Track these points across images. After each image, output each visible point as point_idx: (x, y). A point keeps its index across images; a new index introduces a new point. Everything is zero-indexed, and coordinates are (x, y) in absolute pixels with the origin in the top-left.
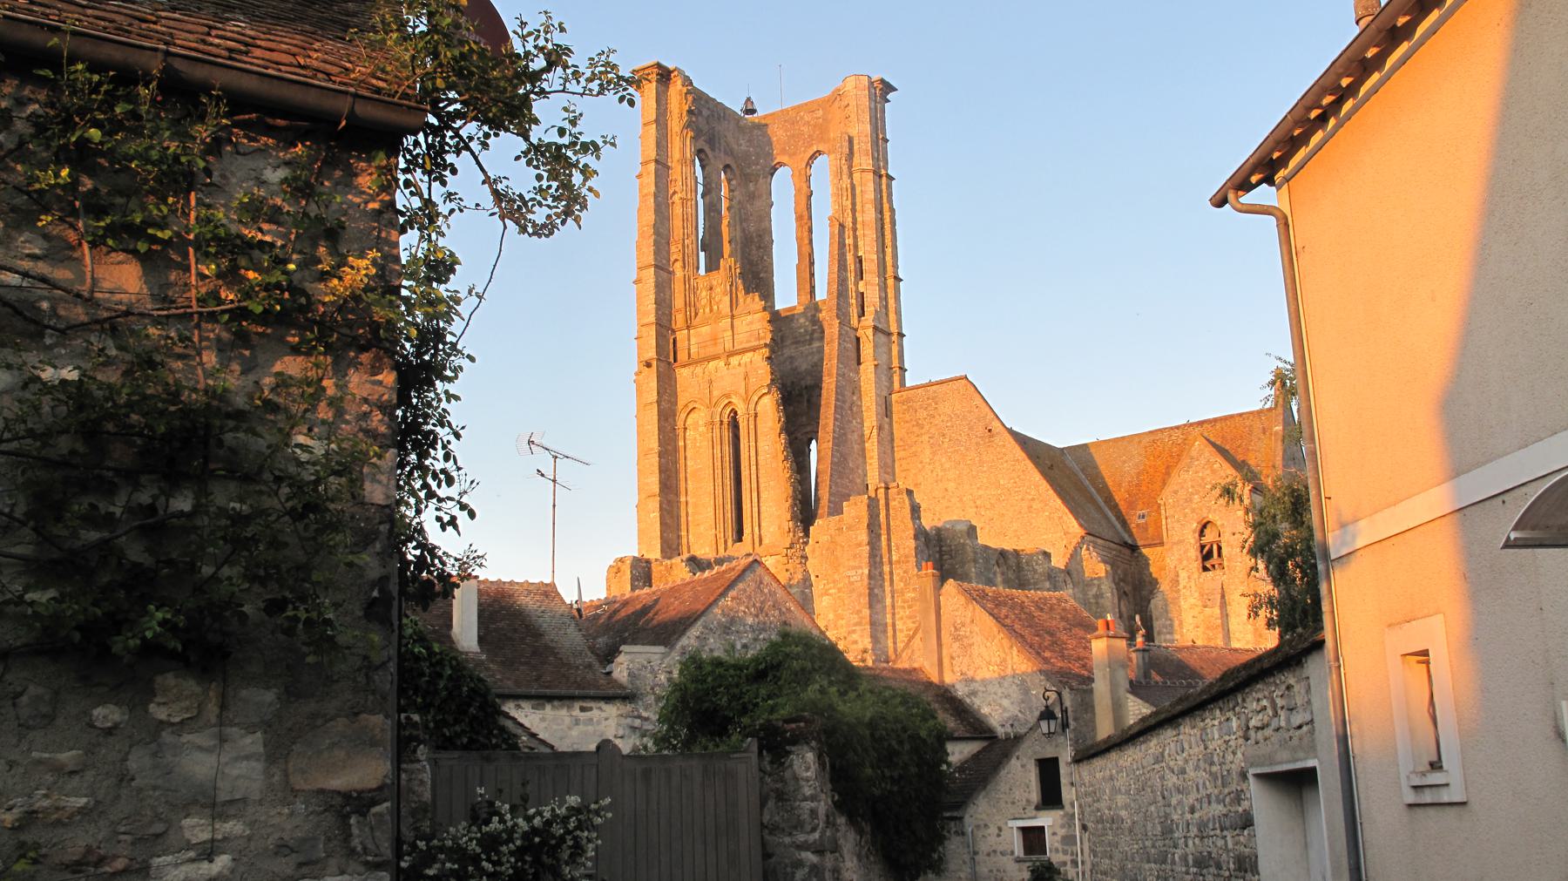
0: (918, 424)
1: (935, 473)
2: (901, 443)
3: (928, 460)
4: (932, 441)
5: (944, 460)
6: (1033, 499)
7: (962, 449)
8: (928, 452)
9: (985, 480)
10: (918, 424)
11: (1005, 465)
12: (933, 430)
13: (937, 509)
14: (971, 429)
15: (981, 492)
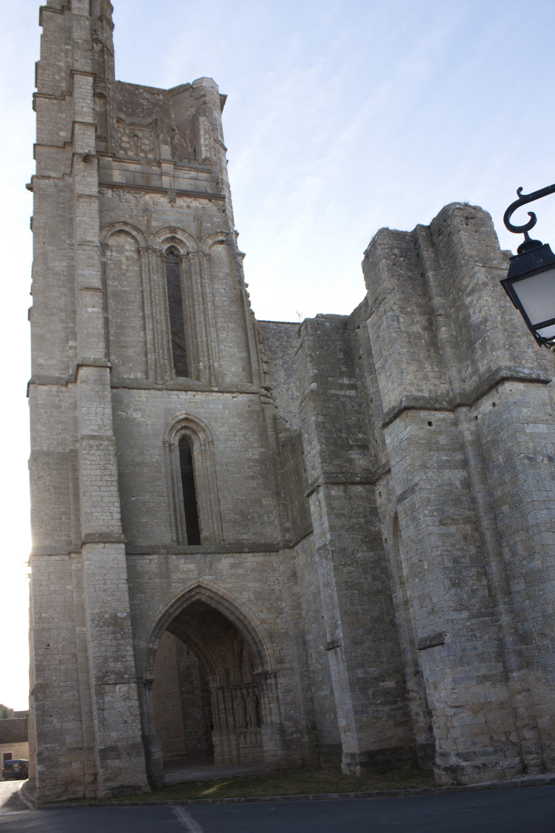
1: (290, 393)
3: (283, 380)
4: (285, 366)
8: (282, 373)
12: (287, 358)
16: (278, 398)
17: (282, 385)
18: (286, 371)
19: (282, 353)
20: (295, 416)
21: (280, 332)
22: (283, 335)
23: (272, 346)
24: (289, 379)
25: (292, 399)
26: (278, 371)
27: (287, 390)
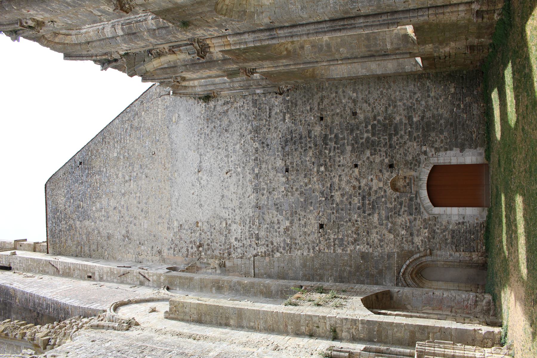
1: (103, 219)
2: (79, 247)
3: (93, 223)
5: (94, 208)
7: (89, 190)
8: (87, 223)
9: (112, 170)
11: (104, 151)
12: (74, 216)
13: (127, 219)
16: (108, 231)
19: (71, 220)
20: (122, 217)
21: (55, 218)
22: (56, 216)
23: (66, 227)
27: (101, 221)
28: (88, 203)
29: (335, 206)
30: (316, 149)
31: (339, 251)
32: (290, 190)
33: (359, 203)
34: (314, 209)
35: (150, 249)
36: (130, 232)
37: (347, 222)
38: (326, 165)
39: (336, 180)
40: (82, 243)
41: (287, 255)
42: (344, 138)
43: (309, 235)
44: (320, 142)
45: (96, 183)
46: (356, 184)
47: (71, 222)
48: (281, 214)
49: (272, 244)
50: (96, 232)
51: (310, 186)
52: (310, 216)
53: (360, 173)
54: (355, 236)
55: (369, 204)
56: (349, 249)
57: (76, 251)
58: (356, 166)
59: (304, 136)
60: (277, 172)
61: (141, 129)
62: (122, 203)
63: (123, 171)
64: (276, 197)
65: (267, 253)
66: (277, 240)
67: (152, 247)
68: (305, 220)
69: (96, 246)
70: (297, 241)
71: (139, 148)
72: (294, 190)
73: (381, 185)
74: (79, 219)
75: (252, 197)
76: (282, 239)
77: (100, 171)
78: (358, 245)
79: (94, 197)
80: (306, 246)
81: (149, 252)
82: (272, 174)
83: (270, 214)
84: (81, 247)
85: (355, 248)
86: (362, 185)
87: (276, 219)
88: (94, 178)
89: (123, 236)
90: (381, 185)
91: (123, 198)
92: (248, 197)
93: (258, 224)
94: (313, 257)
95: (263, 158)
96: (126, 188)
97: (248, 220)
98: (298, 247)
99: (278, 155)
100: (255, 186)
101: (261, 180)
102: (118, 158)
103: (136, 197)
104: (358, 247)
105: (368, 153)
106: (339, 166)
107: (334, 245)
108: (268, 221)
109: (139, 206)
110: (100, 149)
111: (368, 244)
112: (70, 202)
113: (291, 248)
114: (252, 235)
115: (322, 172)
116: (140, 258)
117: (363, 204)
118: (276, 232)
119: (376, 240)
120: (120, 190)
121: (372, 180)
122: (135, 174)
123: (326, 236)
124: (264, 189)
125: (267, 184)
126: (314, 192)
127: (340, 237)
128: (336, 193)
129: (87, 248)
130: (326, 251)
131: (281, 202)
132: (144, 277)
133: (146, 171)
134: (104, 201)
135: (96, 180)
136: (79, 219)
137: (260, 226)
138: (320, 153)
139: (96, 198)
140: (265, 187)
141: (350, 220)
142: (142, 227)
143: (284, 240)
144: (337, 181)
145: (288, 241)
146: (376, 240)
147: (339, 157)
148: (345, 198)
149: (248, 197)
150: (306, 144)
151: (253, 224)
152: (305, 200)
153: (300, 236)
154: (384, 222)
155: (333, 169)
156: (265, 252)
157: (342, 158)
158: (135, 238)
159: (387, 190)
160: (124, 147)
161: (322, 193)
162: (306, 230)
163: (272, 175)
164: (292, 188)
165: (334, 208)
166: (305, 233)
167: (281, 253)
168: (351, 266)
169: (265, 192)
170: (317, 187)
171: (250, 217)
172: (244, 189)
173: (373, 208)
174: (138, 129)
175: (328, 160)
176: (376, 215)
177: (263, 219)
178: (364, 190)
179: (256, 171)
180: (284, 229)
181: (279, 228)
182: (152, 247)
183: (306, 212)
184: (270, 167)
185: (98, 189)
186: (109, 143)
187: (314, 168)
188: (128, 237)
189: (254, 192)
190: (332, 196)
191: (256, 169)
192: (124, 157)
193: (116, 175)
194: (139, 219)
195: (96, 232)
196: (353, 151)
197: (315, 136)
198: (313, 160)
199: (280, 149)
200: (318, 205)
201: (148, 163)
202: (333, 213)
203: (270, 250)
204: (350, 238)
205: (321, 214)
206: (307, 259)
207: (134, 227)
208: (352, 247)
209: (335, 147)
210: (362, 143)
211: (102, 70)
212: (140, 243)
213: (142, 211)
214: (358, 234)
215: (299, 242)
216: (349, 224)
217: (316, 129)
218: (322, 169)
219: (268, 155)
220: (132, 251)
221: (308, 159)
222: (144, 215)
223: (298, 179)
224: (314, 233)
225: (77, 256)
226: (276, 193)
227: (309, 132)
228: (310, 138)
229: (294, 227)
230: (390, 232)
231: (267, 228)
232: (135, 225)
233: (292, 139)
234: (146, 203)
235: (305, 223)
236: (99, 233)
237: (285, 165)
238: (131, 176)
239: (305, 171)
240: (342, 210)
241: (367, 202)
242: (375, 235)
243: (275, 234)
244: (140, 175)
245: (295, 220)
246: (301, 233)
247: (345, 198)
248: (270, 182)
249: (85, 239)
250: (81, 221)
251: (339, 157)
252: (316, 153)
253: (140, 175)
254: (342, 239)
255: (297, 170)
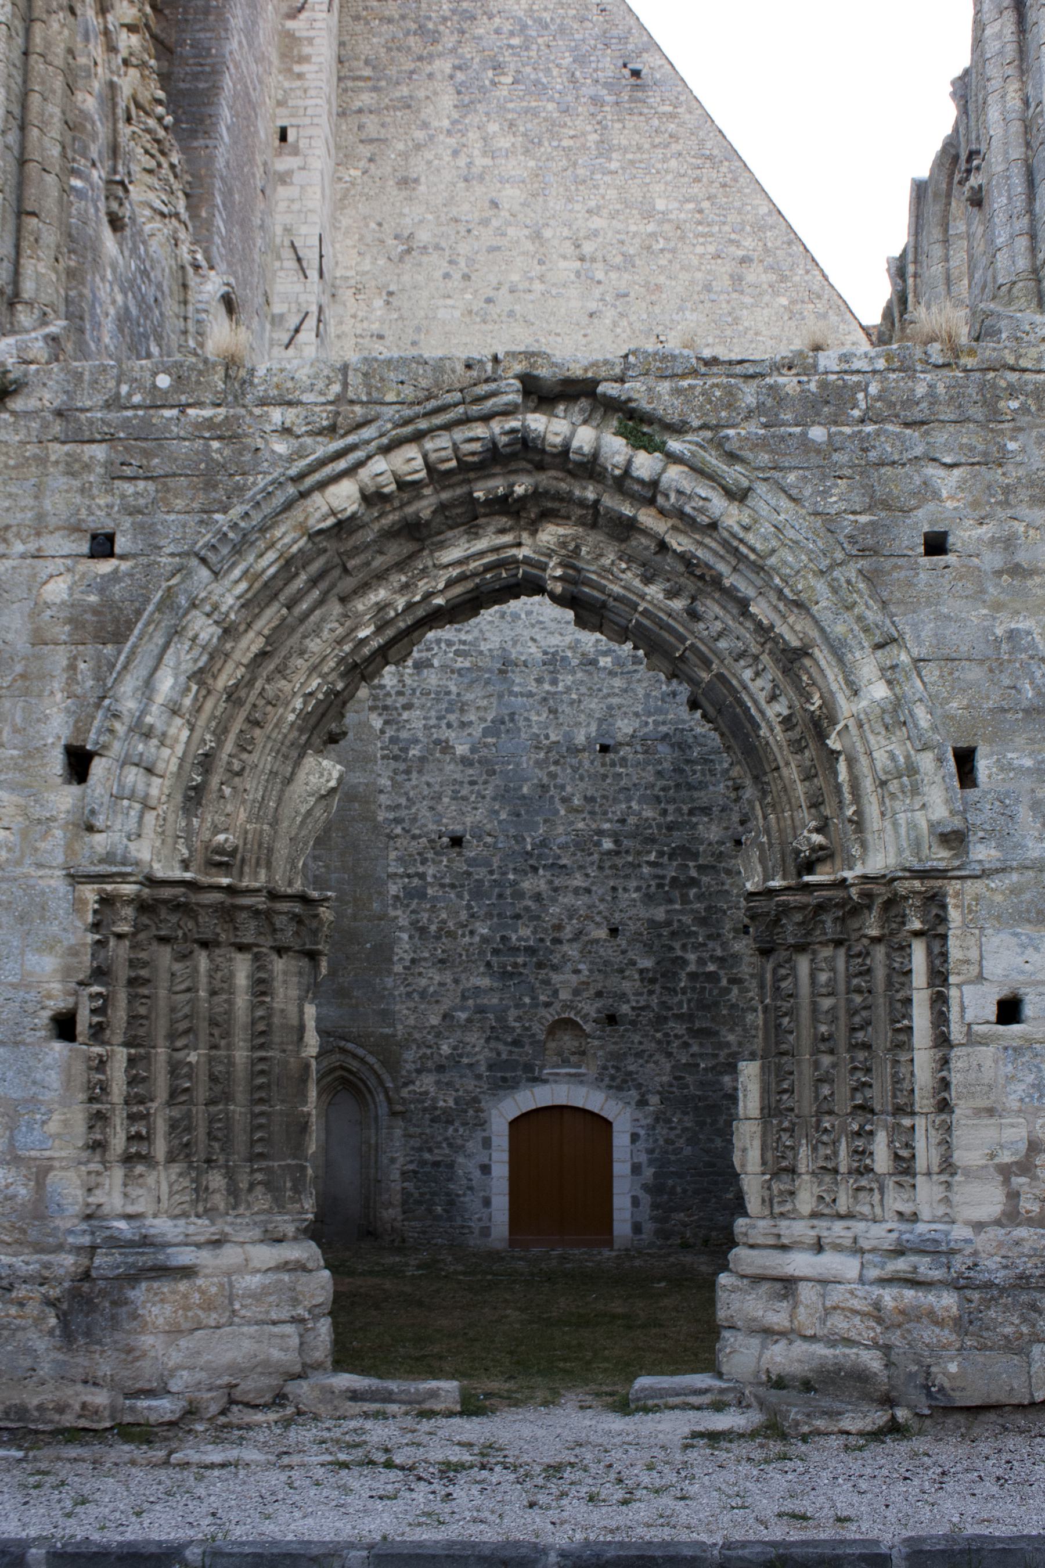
0: (421, 30)
1: (462, 161)
2: (367, 72)
3: (446, 123)
4: (460, 76)
5: (493, 128)
6: (744, 260)
7: (551, 106)
8: (447, 100)
9: (612, 194)
10: (421, 30)
11: (673, 163)
12: (467, 51)
13: (463, 248)
14: (581, 60)
15: (597, 223)
16: (423, 179)
17: (441, 137)
18: (459, 93)
19: (455, 37)
20: (469, 231)
23: (429, 18)
24: (464, 116)
25: (466, 180)
26: (436, 93)
27: (455, 153)
28: (510, 106)
29: (511, 877)
30: (659, 826)
31: (393, 889)
32: (555, 756)
33: (519, 939)
34: (500, 822)
35: (375, 327)
36: (425, 259)
37: (469, 907)
38: (617, 853)
39: (578, 881)
40: (383, 83)
41: (377, 748)
42: (685, 900)
43: (432, 808)
44: (678, 838)
45: (572, 133)
46: (567, 933)
47: (449, 41)
48: (486, 732)
49: (408, 707)
50: (420, 135)
51: (562, 812)
52: (480, 814)
53: (597, 941)
54: (433, 928)
55: (515, 965)
56: (399, 913)
57: (357, 59)
58: (614, 932)
59: (696, 794)
60: (601, 721)
61: (735, 295)
62: (511, 231)
63: (610, 234)
64: (534, 718)
65: (381, 693)
66: (415, 720)
67: (381, 337)
68: (473, 798)
69: (374, 135)
70: (414, 775)
71: (679, 289)
72: (552, 768)
73: (564, 995)
74: (459, 68)
75: (533, 649)
76: (420, 735)
77: (611, 149)
78: (411, 937)
79: (529, 126)
80: (403, 801)
81: (365, 324)
82: (593, 704)
83: (485, 702)
84: (369, 78)
85: (401, 929)
86: (565, 947)
87: (473, 718)
88: (589, 128)
89: (411, 235)
90: (564, 995)
91: (526, 232)
92: (533, 639)
93: (459, 665)
94: (374, 820)
95: (639, 681)
96: (555, 242)
97: (469, 638)
98: (400, 778)
99: (647, 723)
100: (564, 659)
101: (579, 675)
102: (648, 215)
103: (531, 279)
104: (405, 936)
105: (647, 963)
106: (614, 889)
107: (409, 876)
108: (469, 696)
109: (504, 290)
110: (679, 147)
111: (413, 961)
112: (512, 34)
113: (396, 758)
114: (429, 649)
115: (598, 844)
116: (346, 294)
117: (515, 950)
118: (439, 718)
119: (424, 982)
120: (552, 222)
121: (577, 972)
122: (600, 275)
123: (430, 855)
124: (554, 682)
125: (568, 690)
126: (546, 821)
127: (430, 891)
128: (542, 882)
129: (366, 99)
130: (393, 855)
131: (519, 730)
132: (297, 330)
133: (610, 314)
134: (516, 167)
135: (584, 134)
136: (459, 68)
137: (452, 672)
138: (652, 840)
139: (525, 135)
140: (561, 687)
141: (472, 916)
142: (441, 302)
143: (416, 741)
144: (576, 883)
145: (414, 752)
146: (424, 982)
147: (638, 889)
148: (530, 903)
149: (533, 639)
150: (674, 801)
151: (457, 653)
152: (524, 797)
153: (428, 784)
154: (471, 1002)
155: (608, 872)
156: (382, 687)
157: (635, 895)
158: (406, 278)
159: (551, 1010)
160: (682, 238)
161: (544, 843)
162: (446, 800)
163: (593, 706)
164: (556, 763)
165: (505, 874)
166: (438, 797)
167: (383, 732)
168: (354, 917)
169: (547, 687)
170: (561, 829)
171: (474, 643)
172: (553, 626)
173: (505, 975)
174: (737, 280)
175: (630, 859)
176: (485, 982)
177: (472, 682)
178: (552, 952)
179: (605, 662)
180: (447, 741)
181: (449, 726)
182: (381, 337)
183: (494, 799)
184: (615, 701)
185: (555, 143)
186: (697, 180)
187: (610, 821)
188: (409, 251)
189: (545, 653)
190: (535, 869)
191: (609, 659)
192: (653, 235)
193: (599, 207)
194: (463, 290)
195: (420, 135)
196: (653, 924)
197: (694, 827)
198: (632, 820)
199: (664, 729)
200: (512, 832)
201: (633, 318)
202: (491, 872)
203: (389, 702)
204: (426, 915)
205: (489, 840)
206: (367, 802)
207: (438, 274)
208: (403, 921)
209: (663, 877)
210: (671, 949)
211: (914, 180)
212: (390, 294)
213: (489, 300)
214: (438, 938)
215: (414, 782)
216: (464, 915)
217: (714, 828)
218: (608, 844)
219: (647, 696)
220: (367, 266)
221: (634, 805)
222: (475, 309)
223: (582, 779)
224: (438, 823)
225: (340, 62)
226: (543, 718)
227: (706, 811)
228: (691, 813)
229: (452, 767)
230: (445, 1016)
231: (448, 693)
232: (447, 276)
233: (688, 762)
234: (511, 314)
235: (465, 799)
236: (418, 147)
237: (621, 744)
238: (593, 260)
239: (604, 797)
240: (500, 896)
241: (520, 960)
242: (437, 978)
243: (433, 713)
244: (597, 292)
245: (471, 772)
246: (437, 788)
247: (530, 903)
248: (572, 703)
249: (398, 94)
250: (451, 77)
251: (638, 889)
252: (650, 827)
253: (597, 292)
254: (422, 895)
255: (605, 777)
